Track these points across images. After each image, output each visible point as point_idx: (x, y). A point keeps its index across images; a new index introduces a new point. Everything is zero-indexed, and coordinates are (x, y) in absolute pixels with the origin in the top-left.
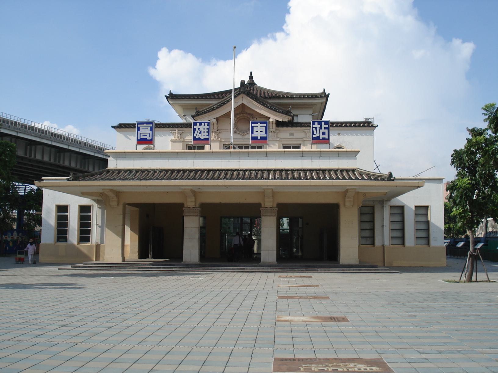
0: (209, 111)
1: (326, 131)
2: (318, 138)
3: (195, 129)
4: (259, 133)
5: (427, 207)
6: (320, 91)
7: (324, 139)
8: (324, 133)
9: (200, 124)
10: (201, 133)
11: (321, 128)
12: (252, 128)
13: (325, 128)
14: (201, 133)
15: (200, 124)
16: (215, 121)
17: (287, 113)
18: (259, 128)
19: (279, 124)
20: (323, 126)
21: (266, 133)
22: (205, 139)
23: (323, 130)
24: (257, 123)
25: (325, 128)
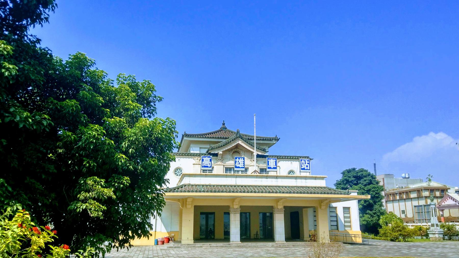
0: (219, 147)
1: (308, 165)
2: (304, 169)
3: (236, 162)
4: (272, 165)
5: (349, 208)
6: (274, 136)
7: (307, 169)
8: (307, 166)
9: (239, 159)
10: (239, 163)
11: (305, 163)
12: (268, 161)
13: (308, 163)
14: (239, 163)
15: (239, 159)
16: (221, 153)
17: (264, 150)
18: (272, 162)
19: (258, 156)
20: (307, 162)
21: (276, 165)
22: (242, 168)
23: (307, 164)
24: (270, 159)
25: (308, 163)
